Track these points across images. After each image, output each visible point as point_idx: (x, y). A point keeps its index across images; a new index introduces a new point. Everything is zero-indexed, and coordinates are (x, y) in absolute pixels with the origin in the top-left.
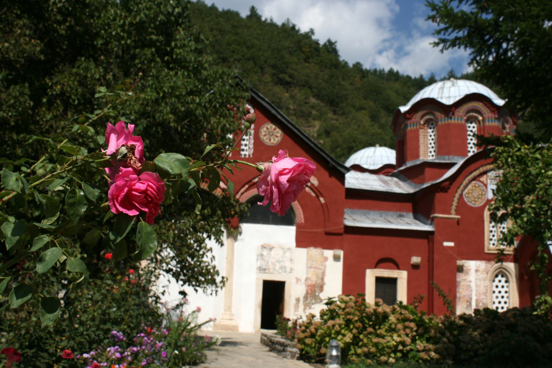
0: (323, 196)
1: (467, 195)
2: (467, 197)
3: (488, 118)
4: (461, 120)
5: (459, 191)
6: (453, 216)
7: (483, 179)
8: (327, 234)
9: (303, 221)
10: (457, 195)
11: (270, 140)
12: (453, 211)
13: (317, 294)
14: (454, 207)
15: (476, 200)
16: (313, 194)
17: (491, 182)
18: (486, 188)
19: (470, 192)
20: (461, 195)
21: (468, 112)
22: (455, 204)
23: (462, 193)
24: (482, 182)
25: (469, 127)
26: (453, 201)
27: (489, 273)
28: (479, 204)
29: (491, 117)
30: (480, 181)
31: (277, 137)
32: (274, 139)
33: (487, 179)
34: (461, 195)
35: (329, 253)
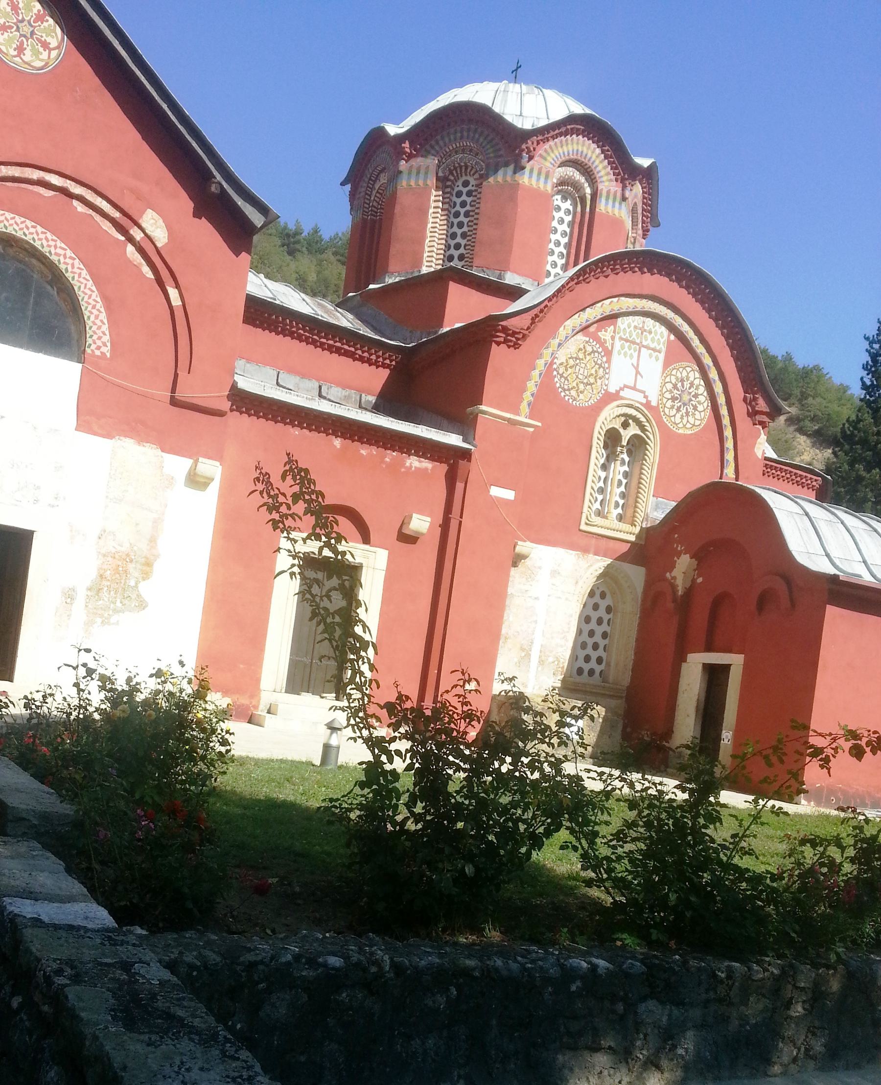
0: (177, 286)
1: (561, 371)
2: (562, 376)
3: (608, 192)
4: (546, 182)
5: (547, 353)
6: (522, 419)
7: (606, 335)
8: (174, 402)
9: (106, 350)
10: (540, 364)
11: (20, 50)
12: (524, 407)
13: (132, 583)
14: (527, 397)
15: (581, 387)
16: (150, 275)
17: (623, 347)
18: (609, 361)
19: (571, 362)
20: (550, 366)
21: (563, 164)
22: (531, 387)
23: (552, 363)
24: (602, 343)
25: (558, 209)
26: (529, 378)
27: (580, 583)
28: (586, 398)
29: (616, 192)
30: (597, 339)
31: (45, 45)
32: (36, 54)
33: (613, 338)
34: (550, 366)
35: (179, 465)
